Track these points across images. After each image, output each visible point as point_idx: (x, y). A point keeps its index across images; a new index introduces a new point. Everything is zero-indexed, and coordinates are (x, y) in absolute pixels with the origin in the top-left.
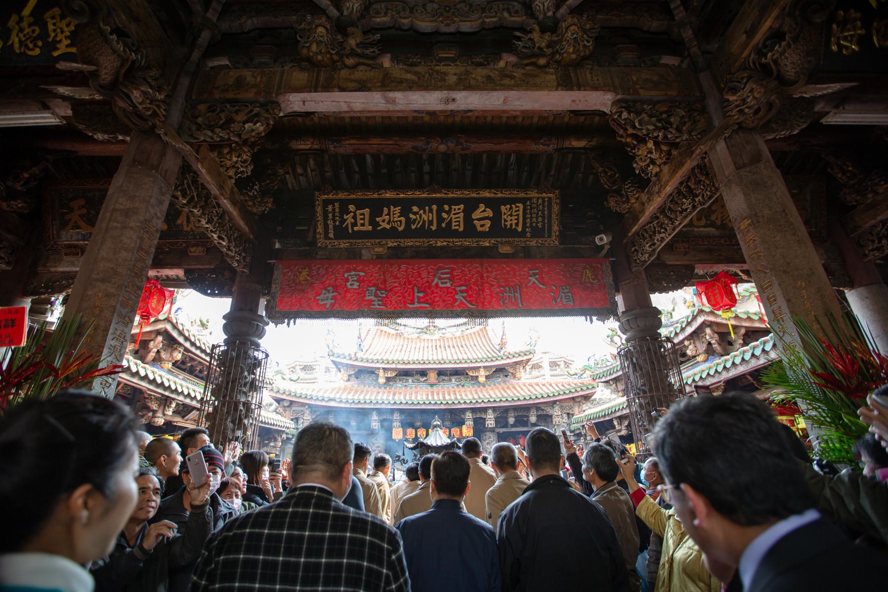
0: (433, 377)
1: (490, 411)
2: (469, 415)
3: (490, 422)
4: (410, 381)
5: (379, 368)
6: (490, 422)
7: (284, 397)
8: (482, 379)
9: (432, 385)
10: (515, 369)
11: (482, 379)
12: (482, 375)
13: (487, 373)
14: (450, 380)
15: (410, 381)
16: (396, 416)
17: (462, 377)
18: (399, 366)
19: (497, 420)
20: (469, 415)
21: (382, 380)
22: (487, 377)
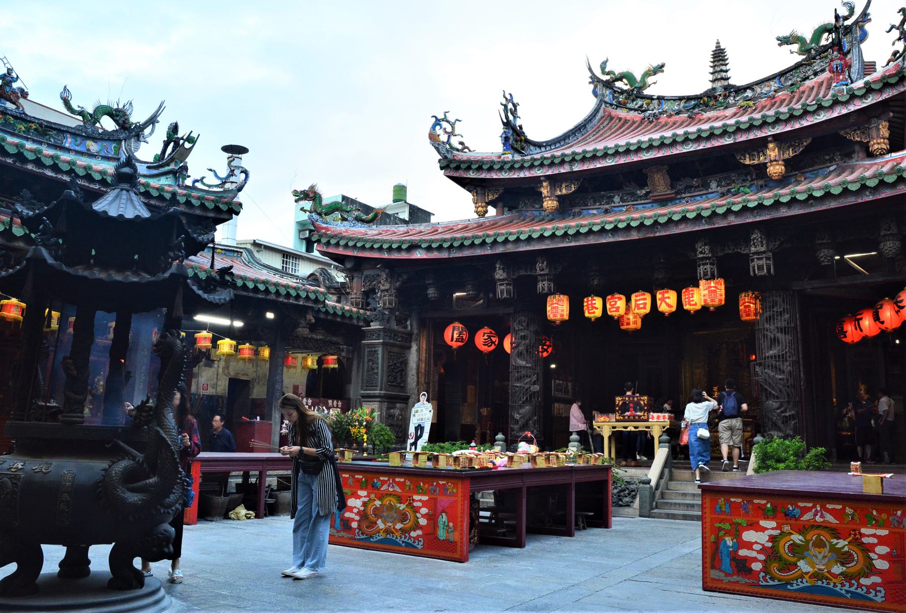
0: (660, 183)
1: (756, 235)
2: (703, 250)
3: (760, 265)
4: (617, 199)
5: (537, 180)
6: (760, 265)
7: (341, 251)
8: (776, 170)
9: (663, 202)
10: (866, 131)
11: (776, 170)
12: (774, 161)
13: (790, 153)
14: (706, 186)
15: (617, 199)
16: (541, 267)
17: (733, 176)
18: (577, 168)
19: (778, 257)
20: (703, 250)
21: (550, 204)
22: (787, 163)
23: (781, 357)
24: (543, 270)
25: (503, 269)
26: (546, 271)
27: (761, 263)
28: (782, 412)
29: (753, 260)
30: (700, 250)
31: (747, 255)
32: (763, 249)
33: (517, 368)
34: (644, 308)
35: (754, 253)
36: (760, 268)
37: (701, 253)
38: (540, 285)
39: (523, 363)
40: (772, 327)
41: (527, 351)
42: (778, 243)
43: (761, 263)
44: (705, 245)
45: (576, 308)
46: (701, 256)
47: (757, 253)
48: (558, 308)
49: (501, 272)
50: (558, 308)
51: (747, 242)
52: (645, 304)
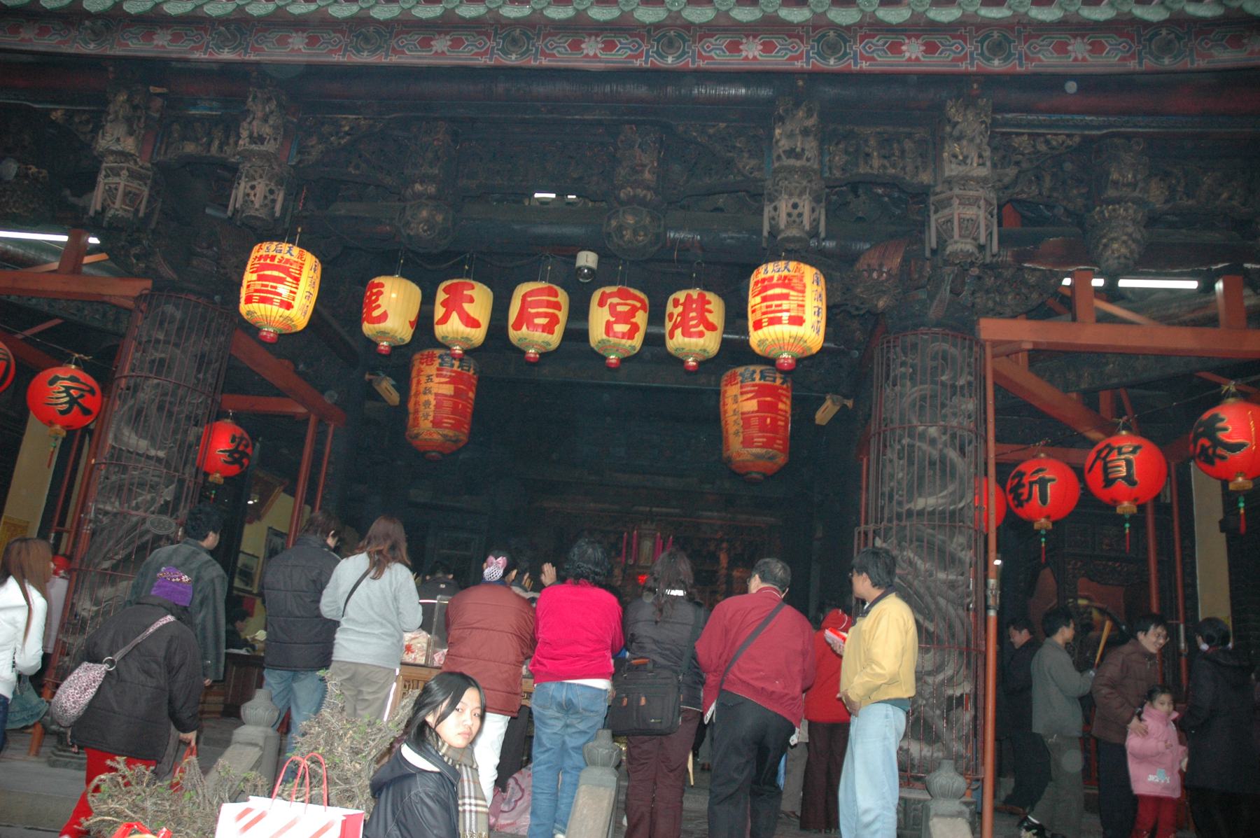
1: (969, 122)
6: (966, 220)
23: (950, 519)
24: (261, 140)
25: (129, 121)
26: (270, 147)
27: (970, 212)
28: (950, 681)
29: (946, 203)
30: (784, 144)
31: (921, 195)
32: (983, 172)
33: (119, 457)
34: (548, 328)
35: (949, 182)
36: (968, 226)
37: (791, 153)
38: (242, 188)
39: (143, 444)
40: (933, 431)
41: (160, 408)
42: (1012, 172)
43: (970, 212)
44: (805, 132)
45: (342, 299)
46: (792, 162)
47: (965, 181)
48: (283, 291)
49: (121, 130)
50: (283, 291)
51: (931, 152)
52: (554, 320)
